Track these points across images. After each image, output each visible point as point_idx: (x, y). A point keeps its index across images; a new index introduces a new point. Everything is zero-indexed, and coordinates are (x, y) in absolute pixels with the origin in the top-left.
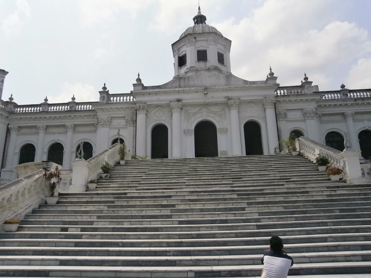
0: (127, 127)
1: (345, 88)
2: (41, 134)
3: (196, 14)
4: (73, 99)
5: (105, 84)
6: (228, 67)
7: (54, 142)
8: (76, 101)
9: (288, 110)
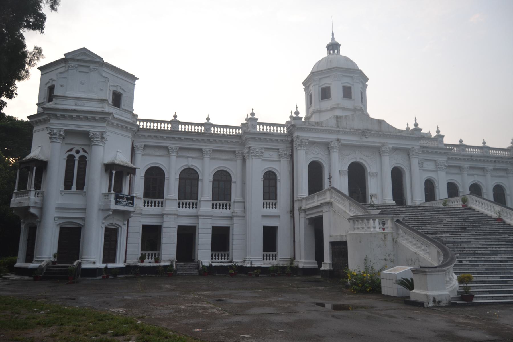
0: (280, 161)
1: (463, 143)
2: (173, 158)
3: (329, 41)
4: (208, 119)
5: (253, 110)
7: (187, 167)
8: (213, 121)
9: (426, 160)
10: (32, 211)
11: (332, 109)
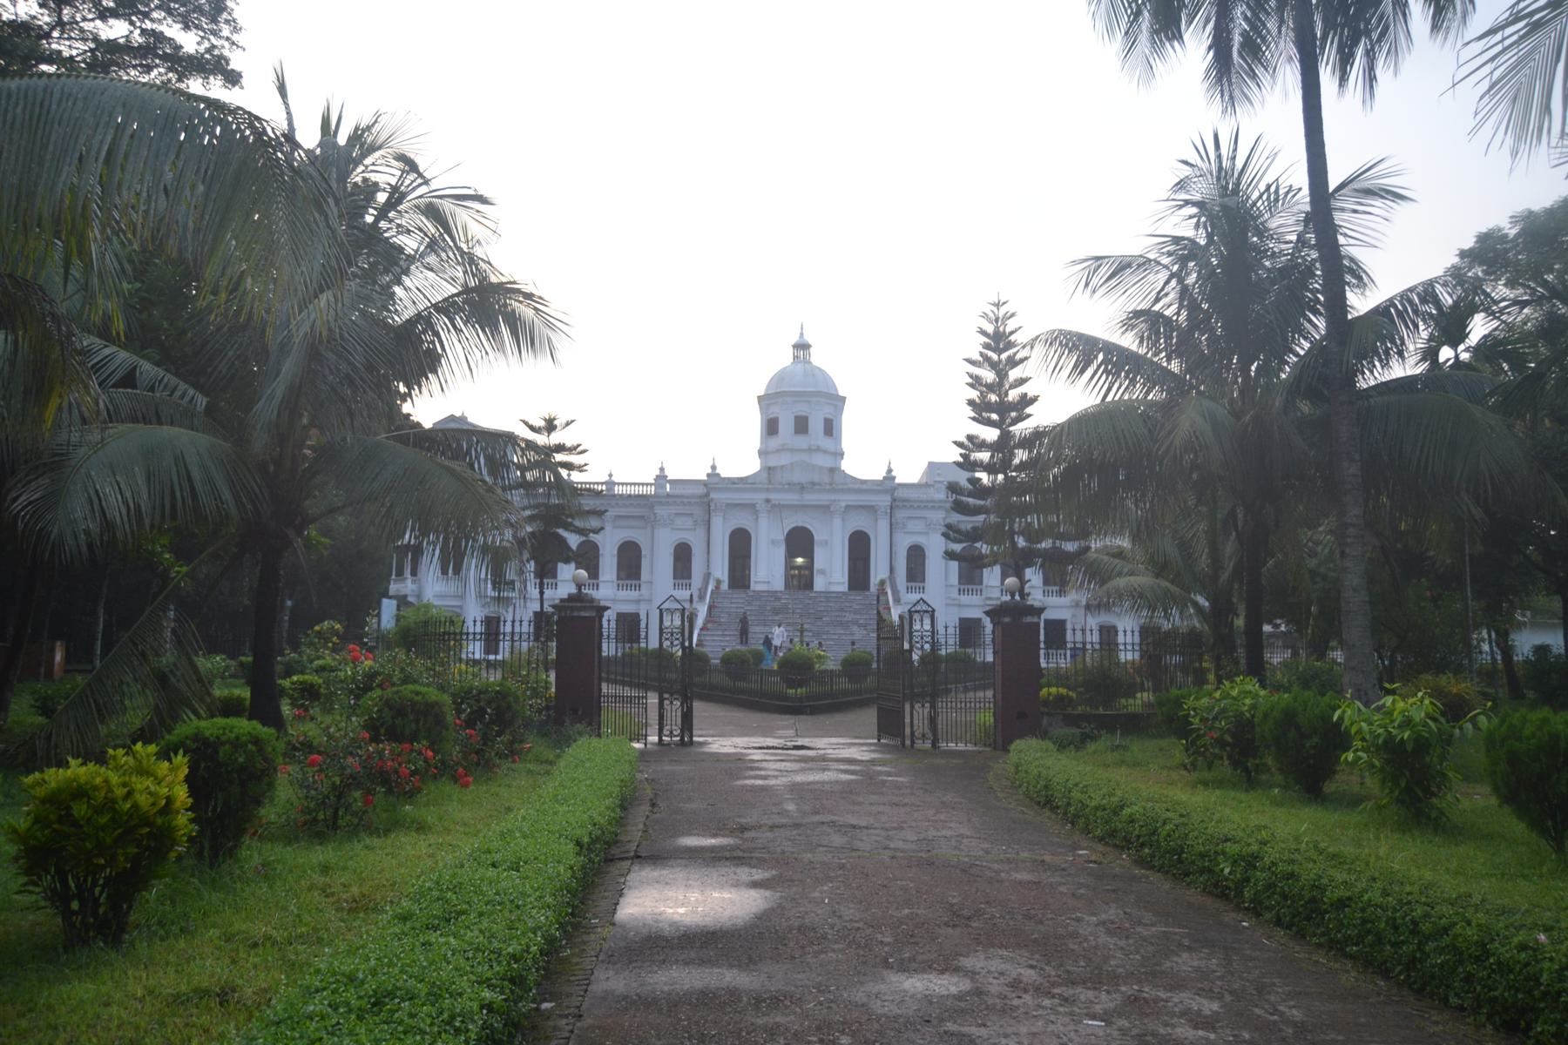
3: (795, 339)
6: (838, 440)
8: (615, 479)
10: (410, 599)
11: (778, 451)
